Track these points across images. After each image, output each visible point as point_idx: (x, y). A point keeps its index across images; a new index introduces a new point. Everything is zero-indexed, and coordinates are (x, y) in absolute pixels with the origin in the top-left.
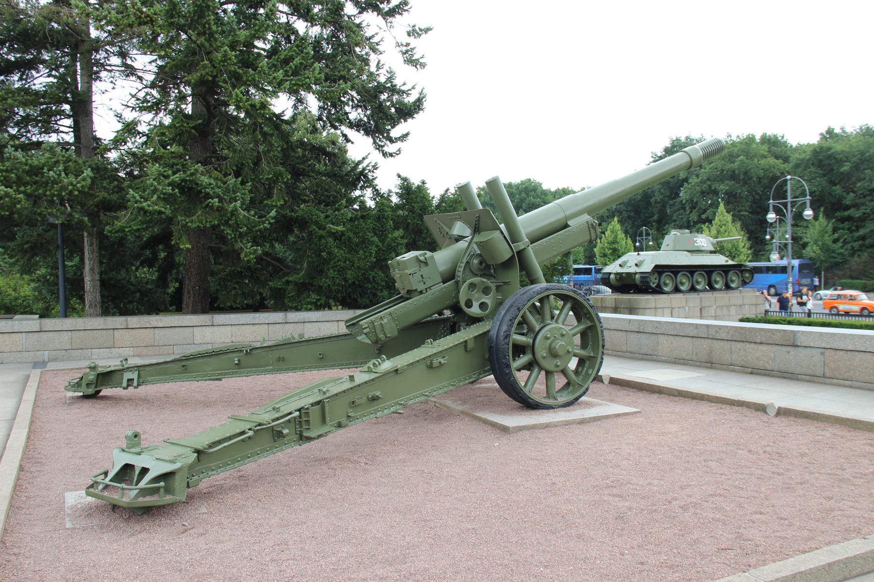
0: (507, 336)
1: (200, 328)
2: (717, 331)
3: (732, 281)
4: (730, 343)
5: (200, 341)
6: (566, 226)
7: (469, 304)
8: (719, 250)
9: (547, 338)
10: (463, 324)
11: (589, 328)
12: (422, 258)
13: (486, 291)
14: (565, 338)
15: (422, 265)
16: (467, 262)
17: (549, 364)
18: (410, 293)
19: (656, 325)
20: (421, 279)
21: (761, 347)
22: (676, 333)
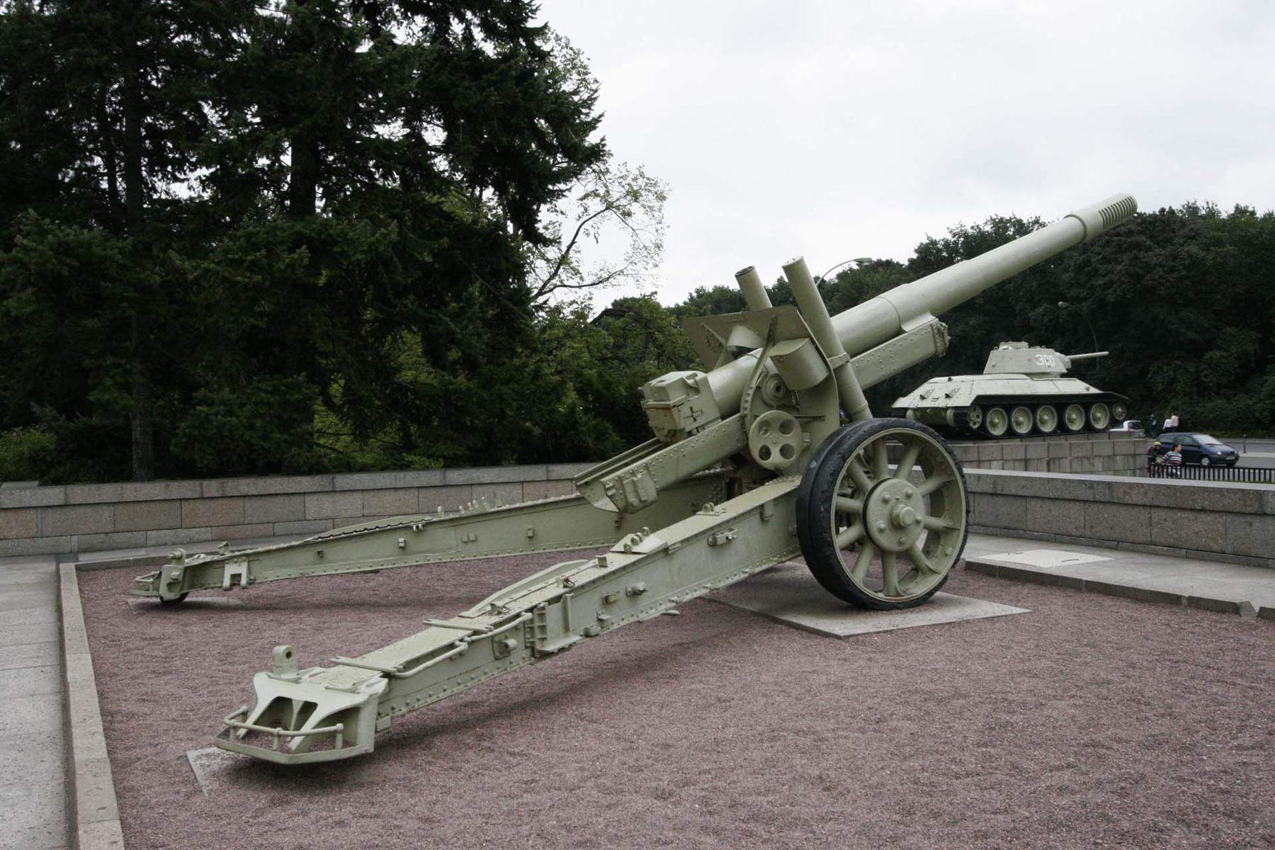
1: (315, 497)
2: (1125, 492)
5: (316, 516)
6: (900, 332)
7: (766, 453)
8: (1074, 372)
9: (886, 501)
12: (690, 382)
13: (785, 428)
15: (692, 393)
16: (758, 388)
17: (887, 541)
18: (675, 435)
19: (1024, 483)
20: (689, 413)
21: (1203, 516)
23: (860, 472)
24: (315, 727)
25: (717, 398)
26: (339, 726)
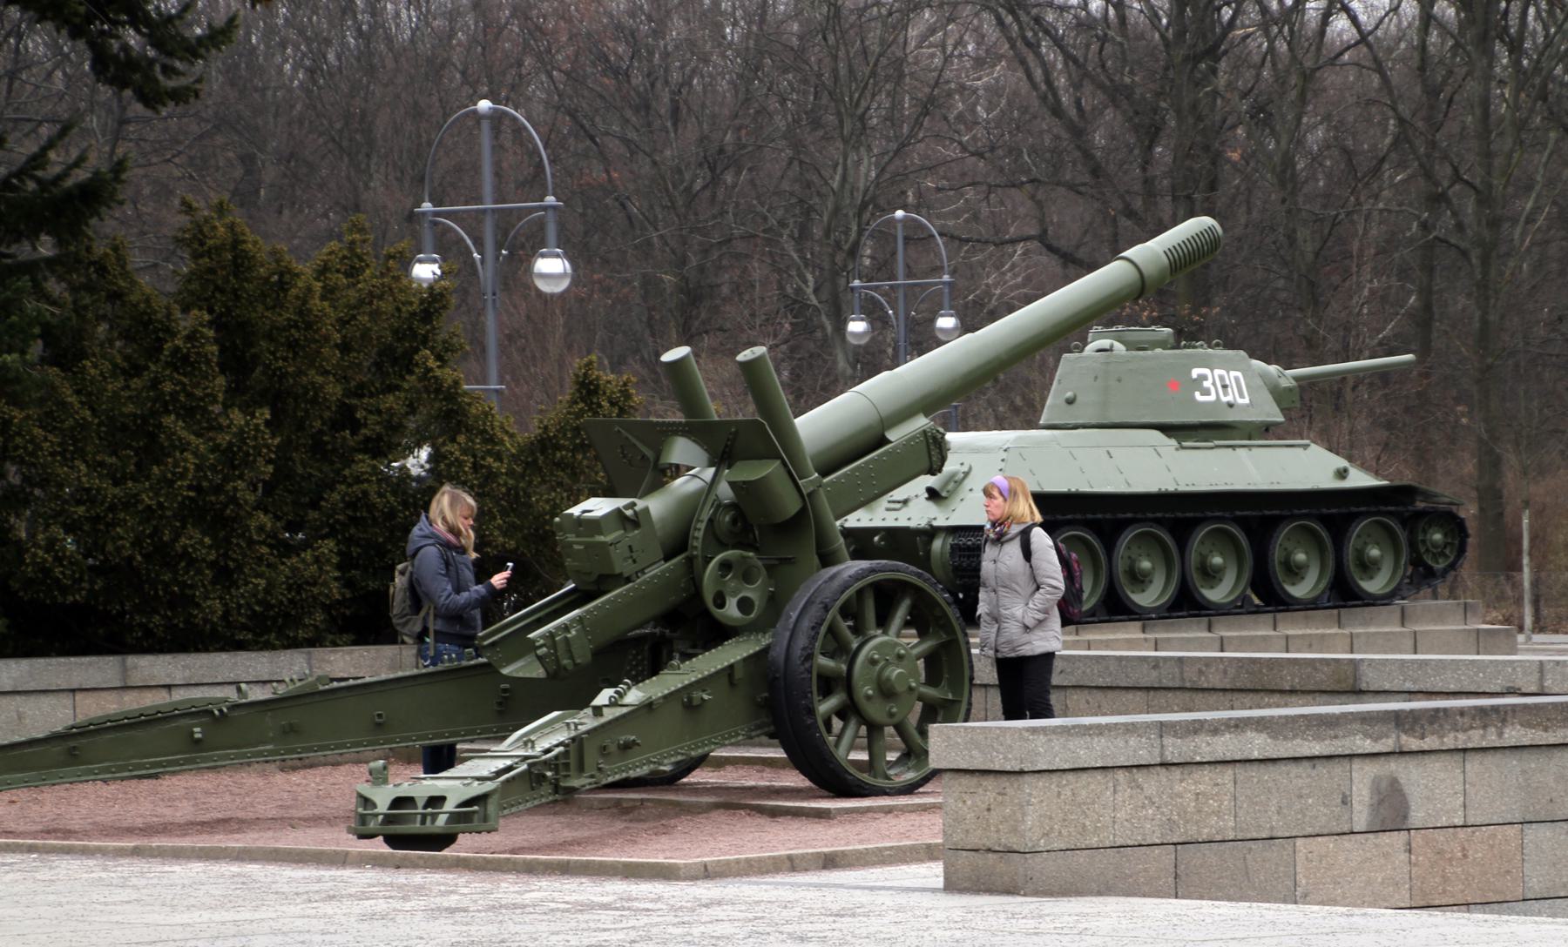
0: (809, 657)
2: (1201, 672)
3: (1368, 567)
4: (1229, 696)
6: (883, 441)
7: (720, 601)
8: (1306, 414)
9: (873, 662)
10: (680, 646)
11: (944, 646)
12: (629, 513)
14: (905, 662)
15: (628, 526)
16: (711, 521)
17: (875, 711)
20: (628, 554)
22: (1108, 681)
23: (844, 626)
24: (460, 806)
25: (659, 534)
26: (476, 808)
